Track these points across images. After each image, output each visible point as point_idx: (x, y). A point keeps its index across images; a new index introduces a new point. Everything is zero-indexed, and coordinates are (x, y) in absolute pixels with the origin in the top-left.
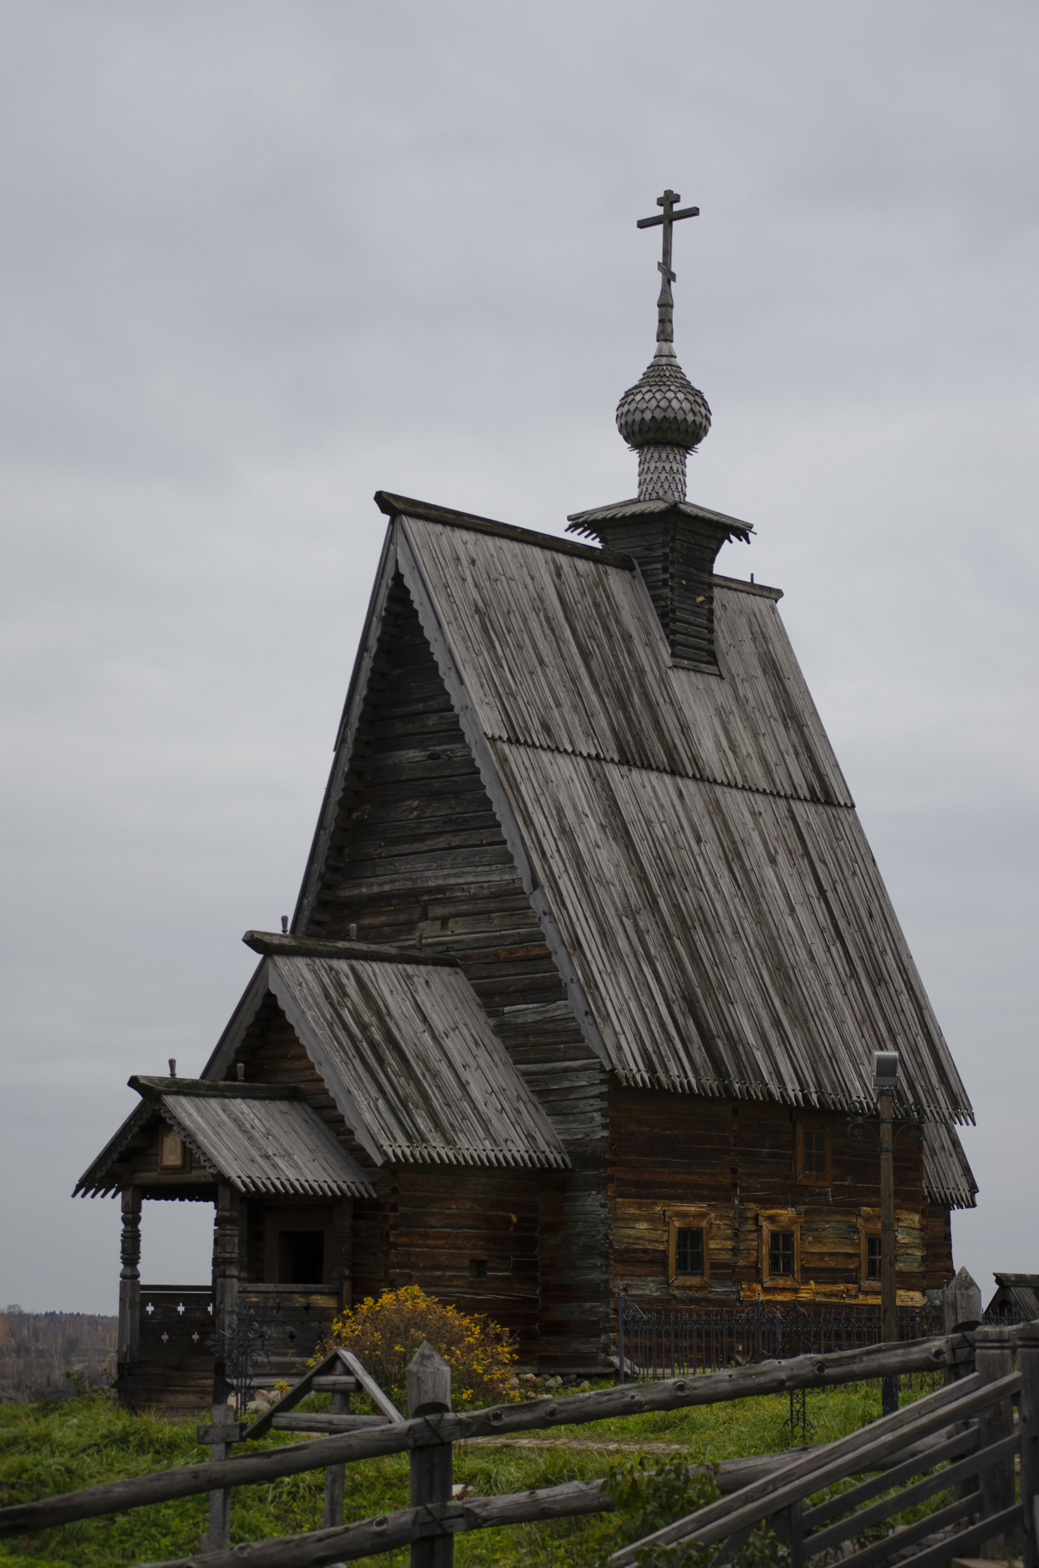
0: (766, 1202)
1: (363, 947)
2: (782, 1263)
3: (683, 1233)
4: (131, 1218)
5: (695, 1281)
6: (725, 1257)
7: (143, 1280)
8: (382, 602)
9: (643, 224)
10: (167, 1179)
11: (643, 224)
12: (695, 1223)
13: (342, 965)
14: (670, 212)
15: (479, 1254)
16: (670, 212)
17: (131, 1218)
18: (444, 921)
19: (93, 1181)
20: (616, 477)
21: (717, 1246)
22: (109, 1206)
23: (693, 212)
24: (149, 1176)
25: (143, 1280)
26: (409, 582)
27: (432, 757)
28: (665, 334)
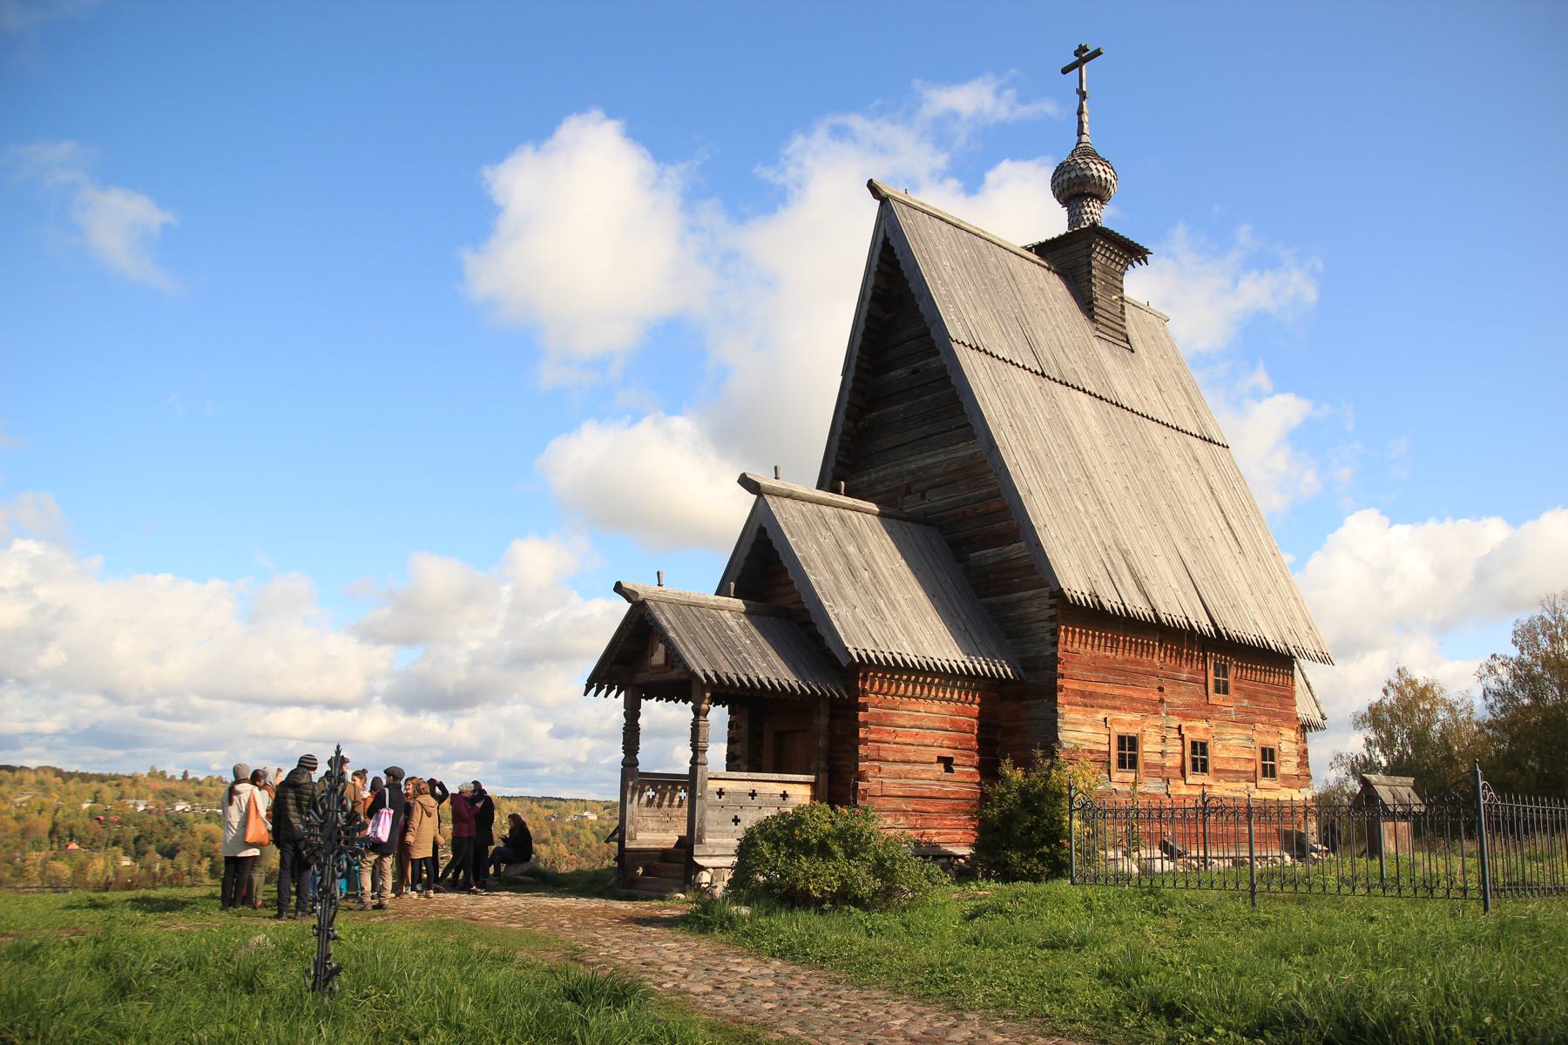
0: (1185, 717)
1: (849, 501)
2: (1201, 766)
3: (1121, 739)
4: (632, 713)
5: (1130, 777)
6: (1156, 758)
7: (642, 768)
8: (876, 261)
9: (1065, 71)
10: (655, 678)
11: (1065, 71)
12: (1132, 732)
13: (828, 510)
14: (1084, 56)
15: (947, 753)
16: (1084, 56)
17: (632, 713)
18: (923, 497)
19: (601, 679)
20: (1053, 222)
21: (1149, 748)
22: (613, 705)
23: (1098, 53)
24: (643, 677)
25: (642, 768)
26: (892, 242)
27: (915, 372)
28: (1080, 133)
